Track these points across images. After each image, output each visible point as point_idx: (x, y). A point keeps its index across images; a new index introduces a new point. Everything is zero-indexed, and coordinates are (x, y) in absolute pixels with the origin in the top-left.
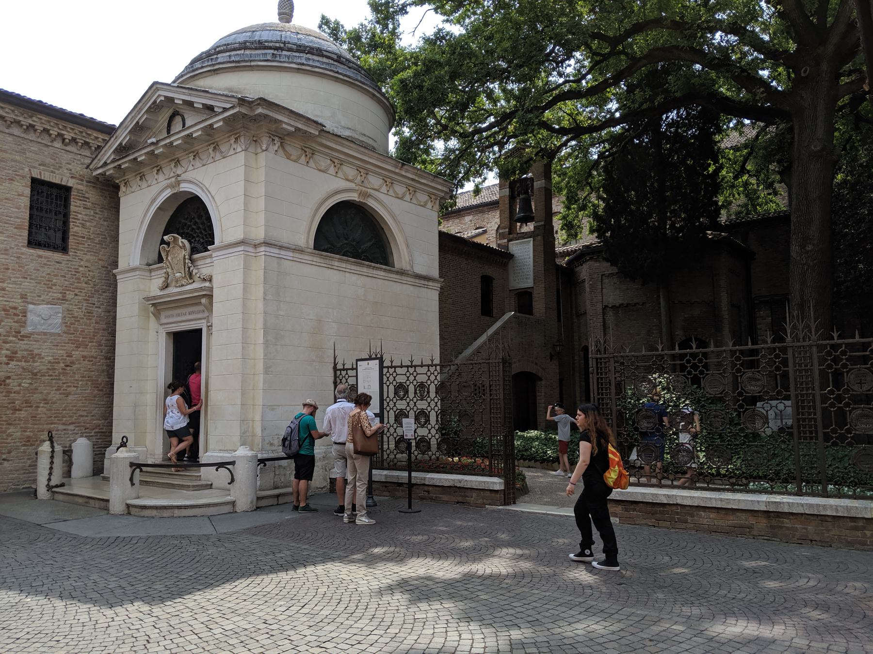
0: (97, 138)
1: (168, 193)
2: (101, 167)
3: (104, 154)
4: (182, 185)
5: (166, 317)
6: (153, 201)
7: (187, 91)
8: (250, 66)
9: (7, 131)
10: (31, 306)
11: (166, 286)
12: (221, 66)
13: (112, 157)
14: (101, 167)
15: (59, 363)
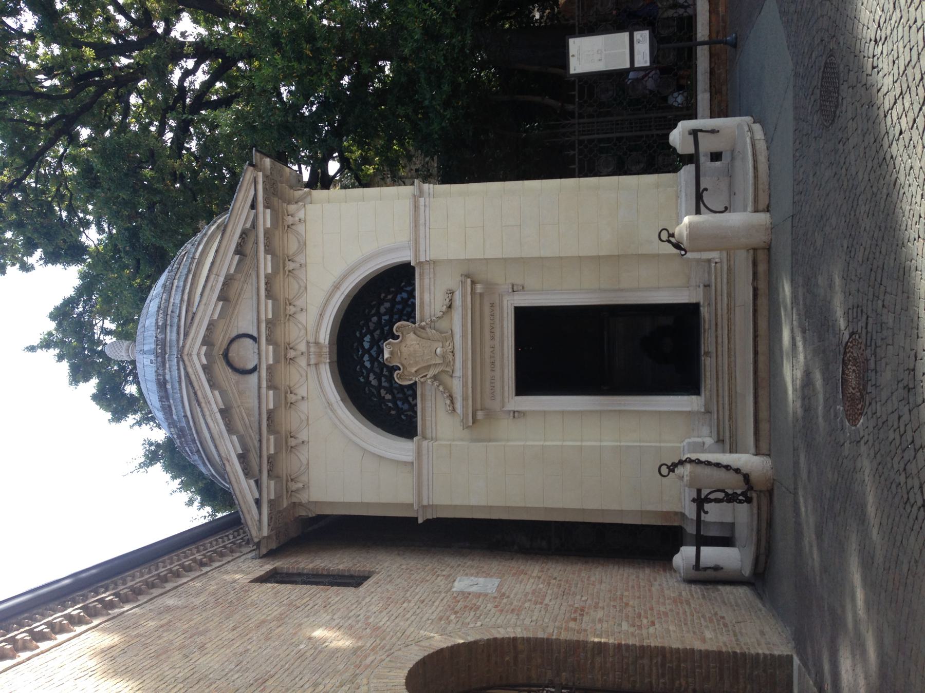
0: (211, 543)
1: (326, 373)
2: (260, 514)
3: (244, 497)
4: (321, 340)
5: (493, 397)
6: (329, 404)
7: (212, 277)
8: (198, 263)
9: (168, 588)
10: (454, 589)
11: (451, 397)
12: (187, 291)
13: (252, 482)
14: (260, 514)
15: (549, 584)
